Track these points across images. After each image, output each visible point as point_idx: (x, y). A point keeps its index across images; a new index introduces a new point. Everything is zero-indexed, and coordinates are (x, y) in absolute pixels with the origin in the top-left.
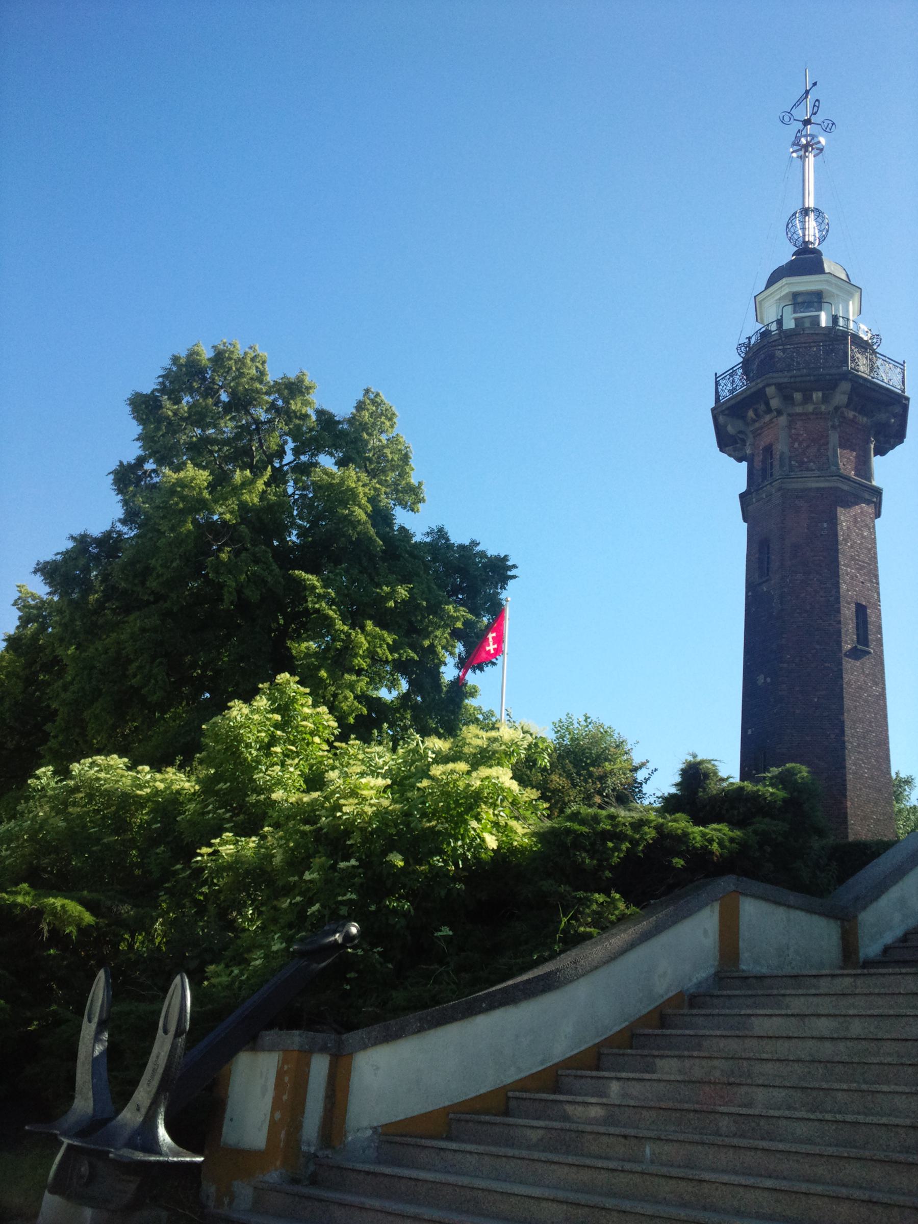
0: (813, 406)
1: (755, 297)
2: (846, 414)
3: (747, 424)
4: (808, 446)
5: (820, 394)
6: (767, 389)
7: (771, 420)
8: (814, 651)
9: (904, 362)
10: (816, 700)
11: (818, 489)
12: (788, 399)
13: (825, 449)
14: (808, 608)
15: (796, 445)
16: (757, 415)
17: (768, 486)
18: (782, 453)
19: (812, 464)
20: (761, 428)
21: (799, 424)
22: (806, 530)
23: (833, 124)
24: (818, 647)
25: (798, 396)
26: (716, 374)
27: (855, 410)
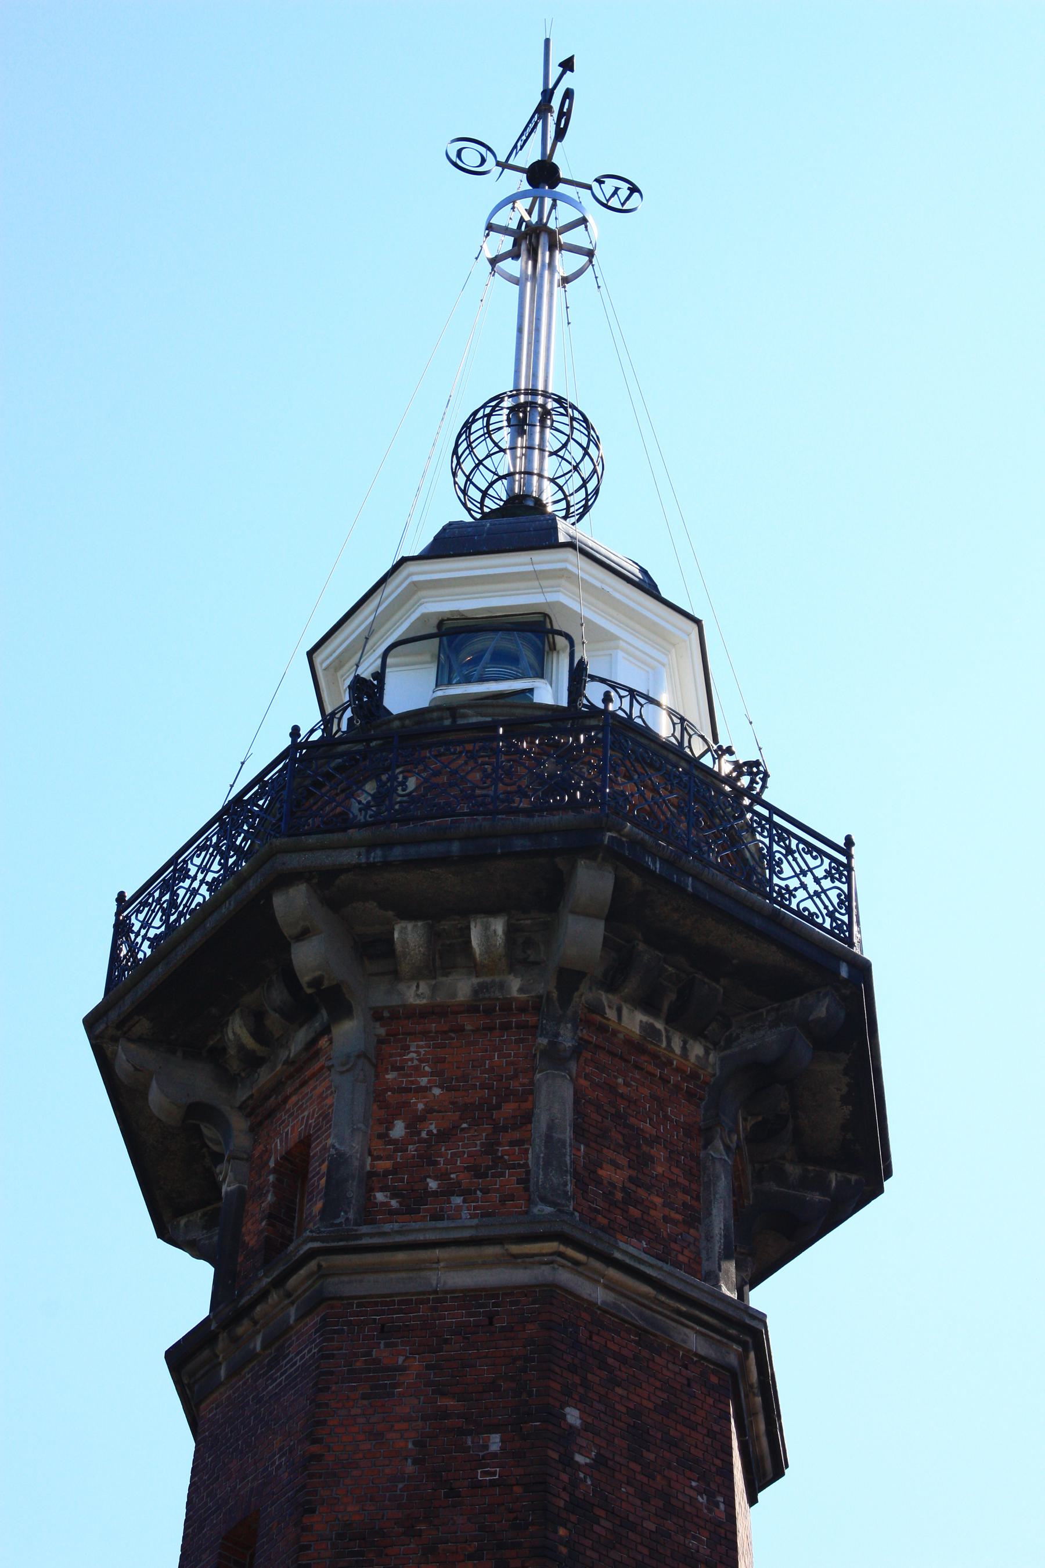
0: (475, 981)
2: (611, 1014)
3: (229, 1081)
4: (445, 1135)
6: (279, 901)
7: (314, 1041)
9: (849, 841)
11: (471, 1297)
13: (512, 1143)
15: (399, 1130)
16: (259, 1033)
17: (274, 1297)
18: (338, 1161)
19: (458, 1200)
20: (277, 1086)
21: (415, 1052)
22: (410, 1468)
23: (634, 189)
26: (121, 896)
27: (648, 1003)
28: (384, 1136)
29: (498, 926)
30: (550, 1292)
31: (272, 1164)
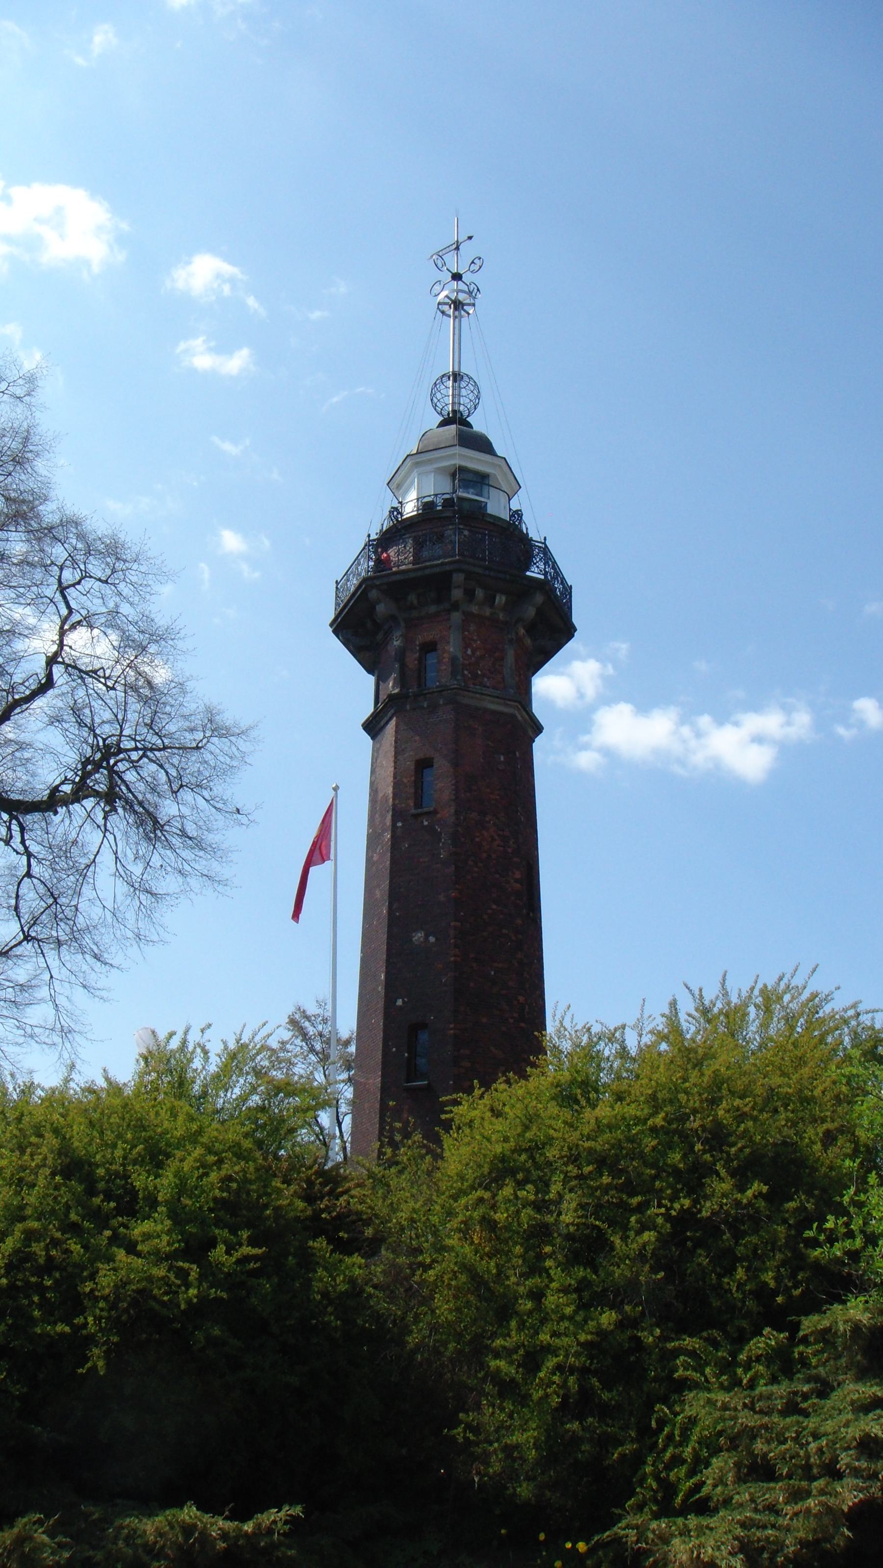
1: (408, 456)
5: (504, 598)
6: (455, 576)
8: (490, 911)
10: (493, 973)
11: (493, 712)
12: (470, 594)
14: (485, 855)
22: (482, 760)
23: (478, 290)
24: (494, 907)
25: (480, 593)
28: (465, 652)
29: (504, 598)
30: (513, 716)
31: (417, 643)
